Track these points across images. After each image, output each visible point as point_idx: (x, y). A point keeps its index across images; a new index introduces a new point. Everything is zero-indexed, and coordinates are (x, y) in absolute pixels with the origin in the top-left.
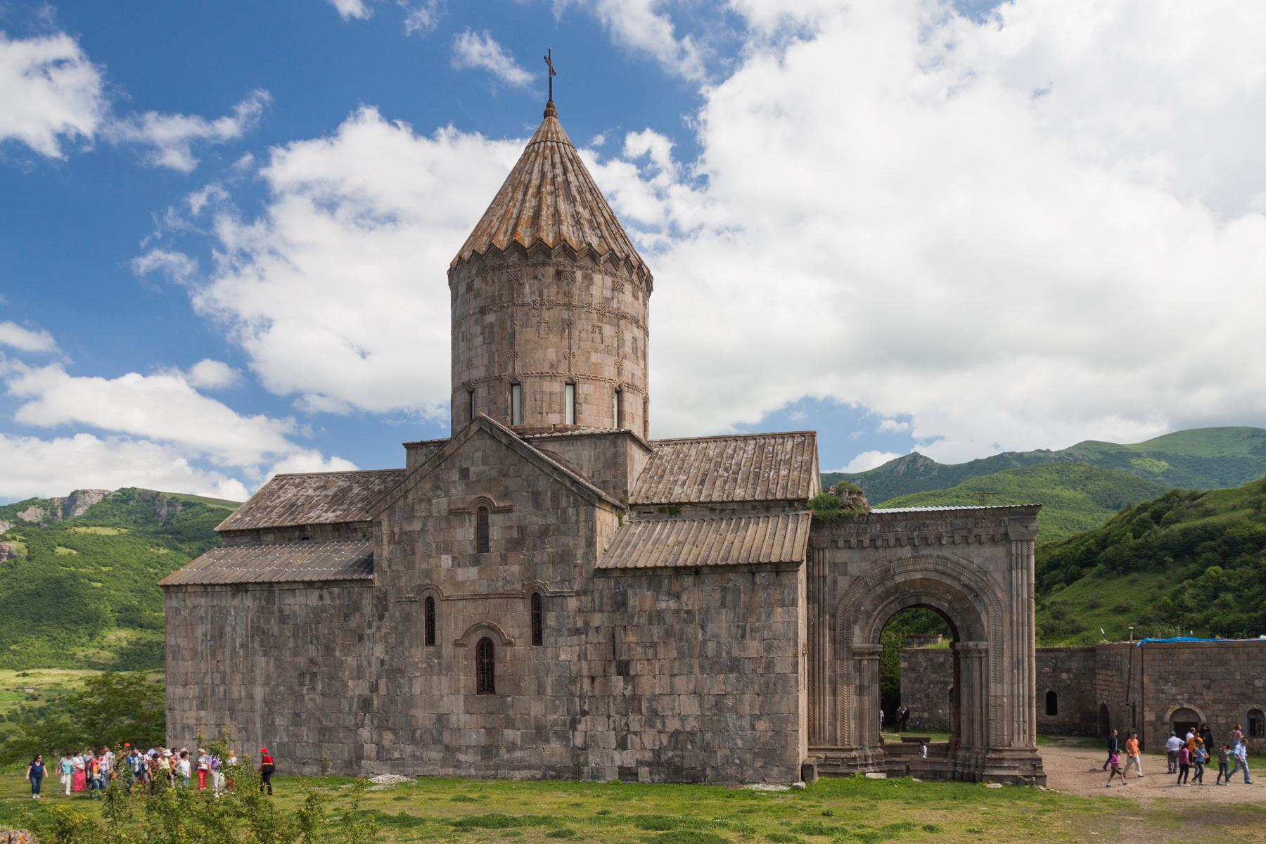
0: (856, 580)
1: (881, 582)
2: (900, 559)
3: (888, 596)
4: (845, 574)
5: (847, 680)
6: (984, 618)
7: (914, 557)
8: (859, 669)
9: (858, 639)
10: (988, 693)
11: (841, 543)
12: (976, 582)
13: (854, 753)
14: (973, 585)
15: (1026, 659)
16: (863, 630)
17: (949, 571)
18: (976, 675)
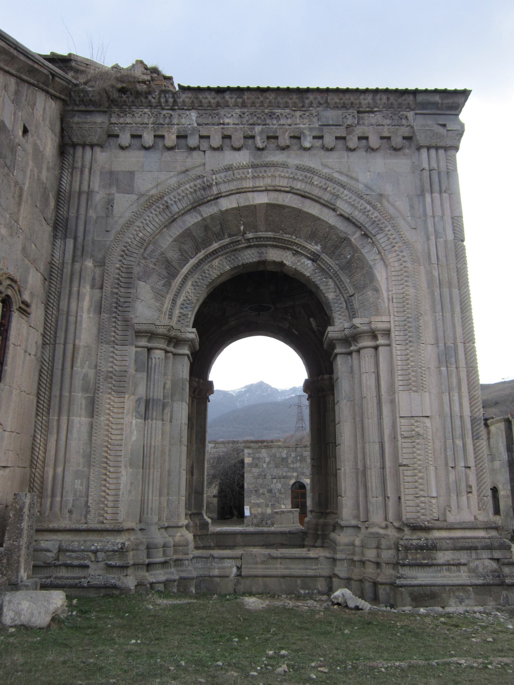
0: (152, 202)
1: (195, 206)
2: (229, 168)
3: (207, 243)
4: (129, 189)
5: (119, 382)
6: (380, 274)
7: (254, 166)
8: (145, 366)
9: (147, 308)
10: (393, 411)
11: (125, 139)
12: (364, 212)
13: (120, 539)
14: (358, 216)
15: (461, 346)
16: (159, 296)
17: (316, 192)
18: (368, 381)
